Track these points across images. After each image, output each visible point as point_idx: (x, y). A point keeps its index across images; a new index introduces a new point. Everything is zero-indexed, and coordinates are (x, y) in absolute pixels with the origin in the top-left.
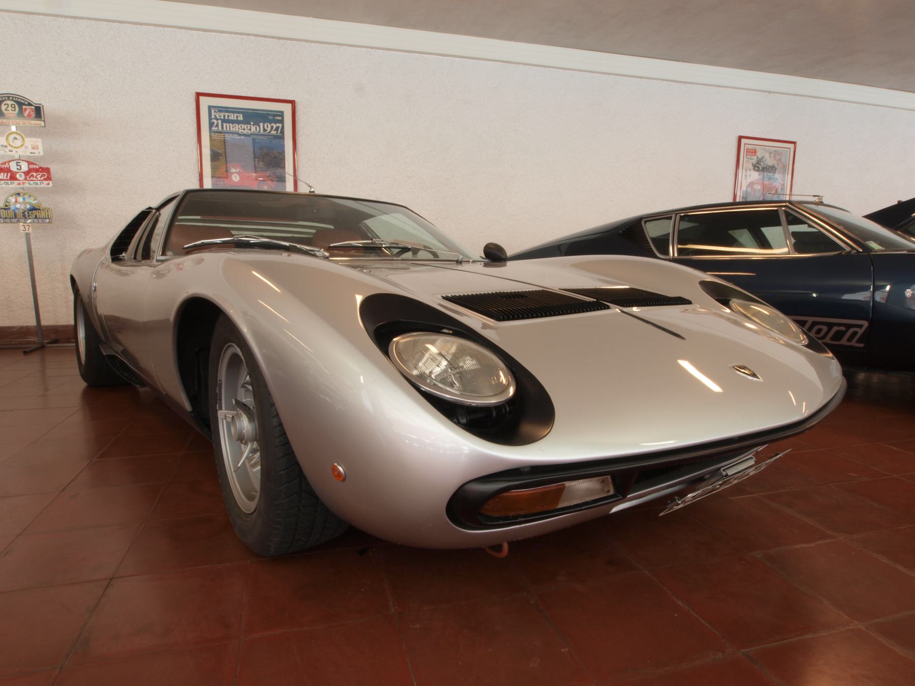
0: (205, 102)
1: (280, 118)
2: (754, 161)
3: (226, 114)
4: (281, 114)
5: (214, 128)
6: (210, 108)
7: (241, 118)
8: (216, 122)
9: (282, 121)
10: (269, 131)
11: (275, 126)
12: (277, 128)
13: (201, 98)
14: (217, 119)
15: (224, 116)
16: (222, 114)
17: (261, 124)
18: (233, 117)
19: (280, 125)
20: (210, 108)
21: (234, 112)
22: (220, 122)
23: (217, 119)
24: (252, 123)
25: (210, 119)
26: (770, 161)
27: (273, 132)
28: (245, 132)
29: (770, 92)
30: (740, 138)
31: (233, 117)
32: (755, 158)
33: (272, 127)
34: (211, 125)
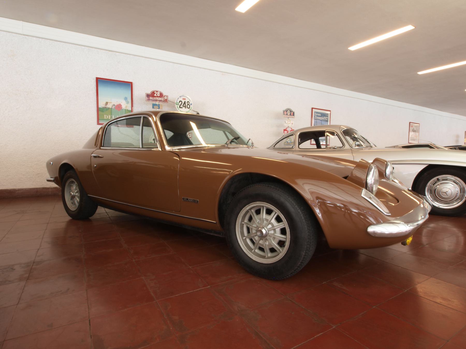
0: (314, 110)
1: (327, 115)
2: (412, 129)
3: (318, 114)
4: (328, 114)
5: (315, 118)
6: (315, 112)
7: (320, 115)
9: (328, 116)
11: (327, 117)
13: (313, 109)
14: (316, 115)
18: (319, 115)
19: (327, 117)
20: (315, 112)
21: (319, 114)
23: (316, 115)
25: (314, 115)
26: (415, 129)
27: (326, 119)
28: (321, 119)
29: (415, 110)
30: (410, 123)
31: (319, 115)
32: (412, 128)
34: (315, 117)
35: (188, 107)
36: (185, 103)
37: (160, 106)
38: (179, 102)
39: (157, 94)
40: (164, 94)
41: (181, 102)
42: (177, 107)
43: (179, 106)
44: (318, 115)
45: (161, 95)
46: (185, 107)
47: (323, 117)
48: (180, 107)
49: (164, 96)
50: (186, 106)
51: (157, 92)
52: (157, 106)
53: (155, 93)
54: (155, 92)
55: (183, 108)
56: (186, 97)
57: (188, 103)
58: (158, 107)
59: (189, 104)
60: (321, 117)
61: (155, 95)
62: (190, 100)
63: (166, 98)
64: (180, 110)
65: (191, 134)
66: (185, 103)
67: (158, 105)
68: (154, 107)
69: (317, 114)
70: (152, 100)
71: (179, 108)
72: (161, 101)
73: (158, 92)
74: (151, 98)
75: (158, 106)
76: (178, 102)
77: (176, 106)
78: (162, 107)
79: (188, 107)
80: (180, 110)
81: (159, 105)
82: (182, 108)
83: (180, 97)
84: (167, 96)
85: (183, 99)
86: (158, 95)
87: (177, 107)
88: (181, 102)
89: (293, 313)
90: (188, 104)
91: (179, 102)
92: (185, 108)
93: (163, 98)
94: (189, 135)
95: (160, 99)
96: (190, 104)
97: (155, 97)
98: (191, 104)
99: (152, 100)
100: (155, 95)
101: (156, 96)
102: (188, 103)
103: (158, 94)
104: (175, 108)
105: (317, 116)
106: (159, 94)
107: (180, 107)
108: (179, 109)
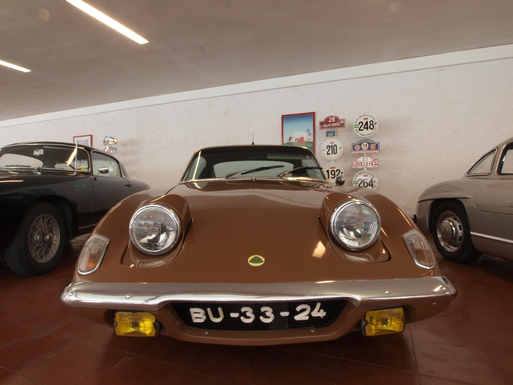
35: (372, 127)
36: (367, 123)
37: (335, 132)
38: (359, 124)
39: (331, 120)
40: (340, 118)
41: (361, 124)
42: (356, 130)
43: (358, 129)
45: (337, 120)
46: (367, 128)
48: (360, 130)
49: (341, 120)
50: (369, 126)
51: (332, 117)
52: (332, 133)
53: (330, 119)
54: (329, 118)
55: (364, 130)
56: (368, 115)
57: (371, 123)
58: (333, 134)
59: (372, 124)
61: (330, 121)
62: (374, 119)
63: (342, 122)
64: (359, 133)
65: (376, 161)
66: (367, 122)
67: (333, 132)
68: (328, 135)
70: (326, 128)
71: (358, 131)
72: (337, 126)
73: (333, 118)
74: (325, 126)
75: (333, 133)
76: (357, 124)
77: (355, 129)
78: (338, 133)
79: (372, 127)
80: (359, 133)
81: (334, 131)
82: (363, 130)
83: (360, 117)
84: (344, 120)
85: (364, 119)
86: (333, 120)
87: (356, 130)
88: (361, 124)
90: (371, 124)
91: (359, 124)
92: (367, 130)
93: (339, 123)
94: (375, 161)
95: (335, 124)
96: (374, 124)
97: (330, 123)
98: (376, 123)
99: (326, 128)
100: (330, 121)
101: (331, 122)
102: (371, 123)
103: (333, 119)
104: (354, 131)
106: (334, 119)
107: (360, 130)
108: (358, 133)
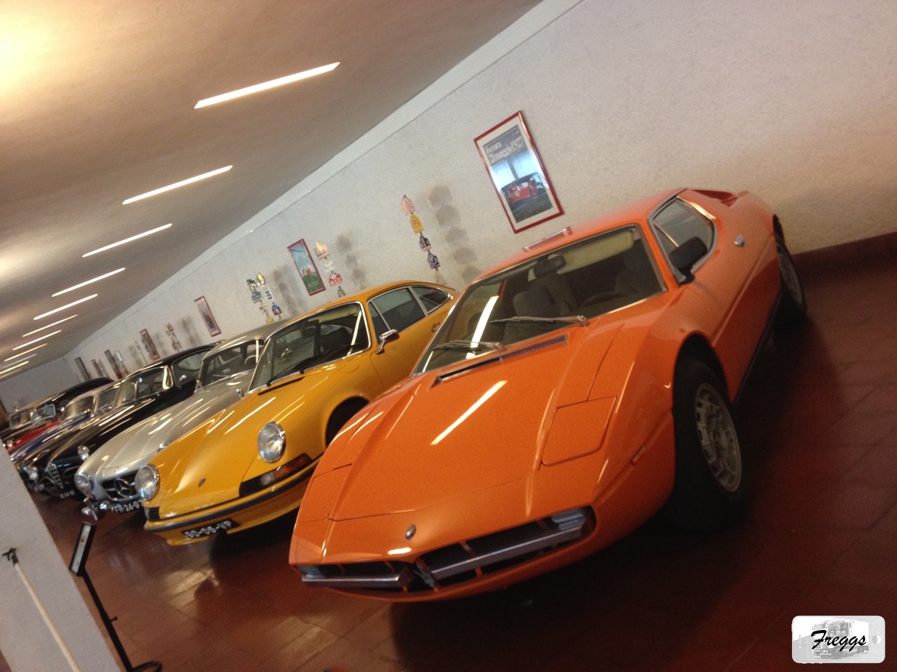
1: (517, 132)
3: (493, 146)
7: (500, 146)
8: (490, 156)
9: (520, 134)
10: (516, 145)
12: (520, 140)
15: (492, 149)
16: (491, 148)
17: (511, 144)
21: (495, 143)
22: (492, 154)
23: (490, 154)
24: (507, 146)
25: (488, 155)
33: (517, 142)
34: (490, 159)
44: (497, 148)
47: (509, 145)
60: (504, 151)
69: (490, 150)
89: (150, 484)
105: (495, 152)
